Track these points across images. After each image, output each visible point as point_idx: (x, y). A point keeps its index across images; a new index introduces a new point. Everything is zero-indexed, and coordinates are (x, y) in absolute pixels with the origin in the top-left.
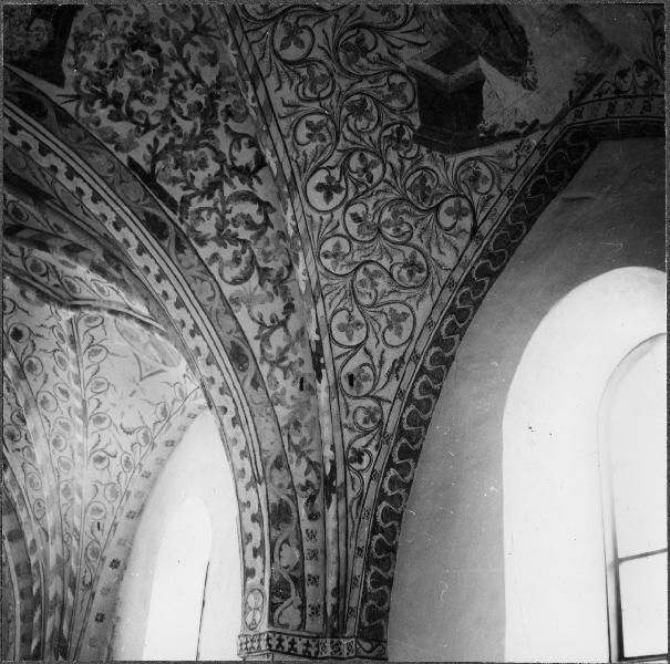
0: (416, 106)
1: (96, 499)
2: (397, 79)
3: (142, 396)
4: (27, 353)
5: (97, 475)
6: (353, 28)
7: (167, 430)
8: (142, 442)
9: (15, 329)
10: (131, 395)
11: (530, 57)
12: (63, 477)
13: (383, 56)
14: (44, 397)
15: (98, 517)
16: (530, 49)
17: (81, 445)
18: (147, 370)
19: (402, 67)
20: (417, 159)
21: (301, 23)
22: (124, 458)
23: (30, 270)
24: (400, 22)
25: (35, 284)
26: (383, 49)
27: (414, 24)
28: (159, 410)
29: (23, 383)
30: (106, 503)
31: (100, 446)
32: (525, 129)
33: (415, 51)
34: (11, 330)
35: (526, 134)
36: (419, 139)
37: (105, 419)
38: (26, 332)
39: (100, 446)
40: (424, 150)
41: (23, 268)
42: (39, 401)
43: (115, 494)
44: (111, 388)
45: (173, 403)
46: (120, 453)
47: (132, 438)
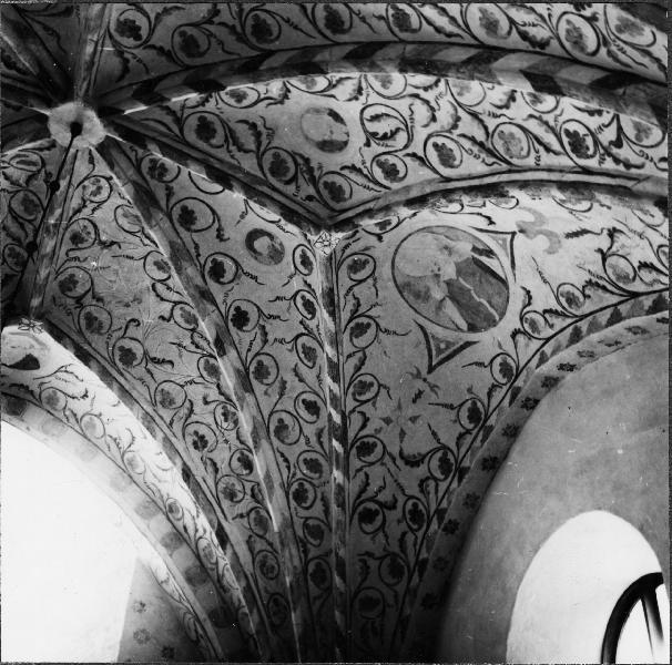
1: (367, 583)
3: (433, 398)
4: (256, 348)
5: (367, 543)
7: (483, 441)
8: (438, 475)
9: (238, 309)
10: (414, 401)
12: (313, 552)
14: (281, 421)
17: (340, 488)
18: (440, 351)
23: (269, 175)
25: (276, 196)
28: (464, 413)
29: (249, 398)
30: (385, 590)
34: (232, 311)
37: (375, 445)
38: (253, 315)
41: (259, 174)
42: (272, 428)
43: (396, 571)
44: (383, 391)
45: (490, 395)
46: (401, 499)
47: (421, 471)
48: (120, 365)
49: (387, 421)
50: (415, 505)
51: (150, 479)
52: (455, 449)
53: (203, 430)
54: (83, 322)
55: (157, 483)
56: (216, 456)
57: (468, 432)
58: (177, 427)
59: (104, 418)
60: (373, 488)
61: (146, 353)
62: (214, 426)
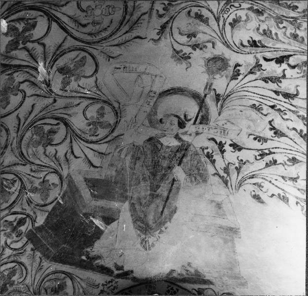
0: (50, 208)
2: (53, 179)
6: (57, 119)
11: (163, 229)
13: (58, 154)
16: (168, 224)
19: (65, 173)
20: (20, 252)
21: (23, 87)
24: (94, 139)
26: (62, 150)
27: (103, 148)
32: (121, 272)
33: (85, 167)
35: (118, 276)
36: (32, 237)
40: (30, 246)
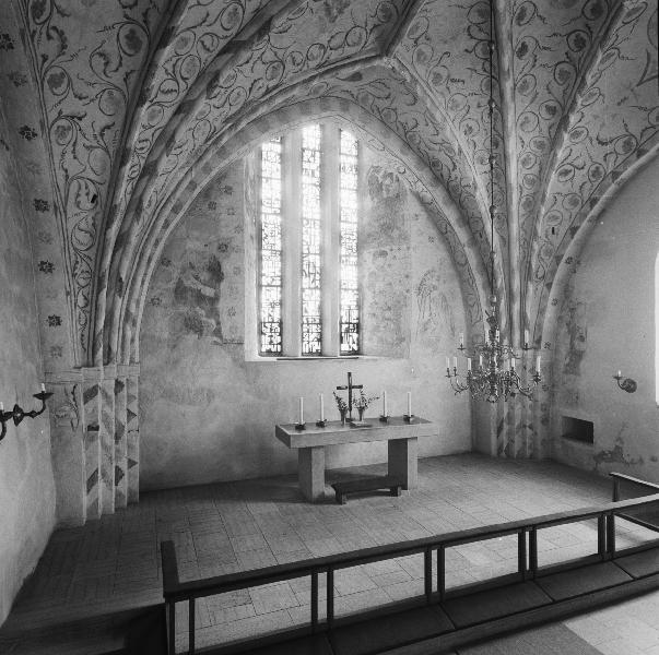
1: (555, 207)
15: (553, 224)
22: (593, 168)
31: (568, 161)
39: (568, 161)
43: (574, 203)
47: (609, 148)
48: (431, 85)
49: (596, 117)
50: (597, 168)
51: (422, 147)
52: (639, 138)
53: (471, 123)
54: (415, 56)
55: (427, 150)
56: (475, 139)
57: (653, 127)
58: (457, 122)
59: (399, 112)
60: (574, 156)
61: (449, 76)
62: (480, 121)
